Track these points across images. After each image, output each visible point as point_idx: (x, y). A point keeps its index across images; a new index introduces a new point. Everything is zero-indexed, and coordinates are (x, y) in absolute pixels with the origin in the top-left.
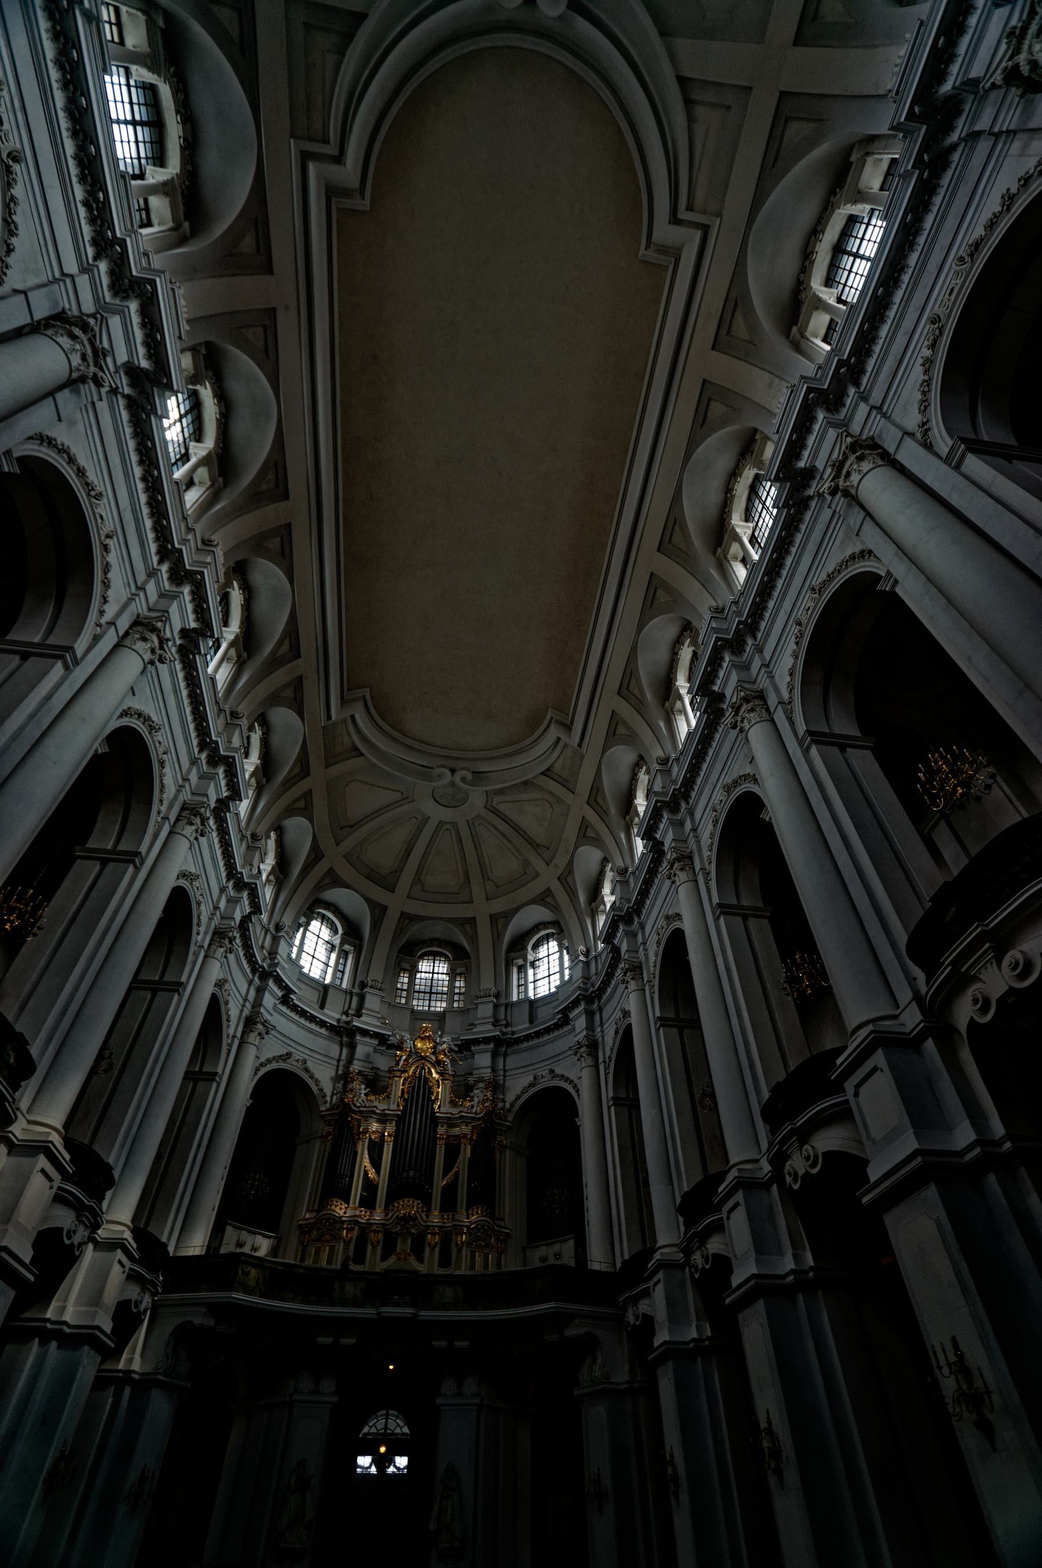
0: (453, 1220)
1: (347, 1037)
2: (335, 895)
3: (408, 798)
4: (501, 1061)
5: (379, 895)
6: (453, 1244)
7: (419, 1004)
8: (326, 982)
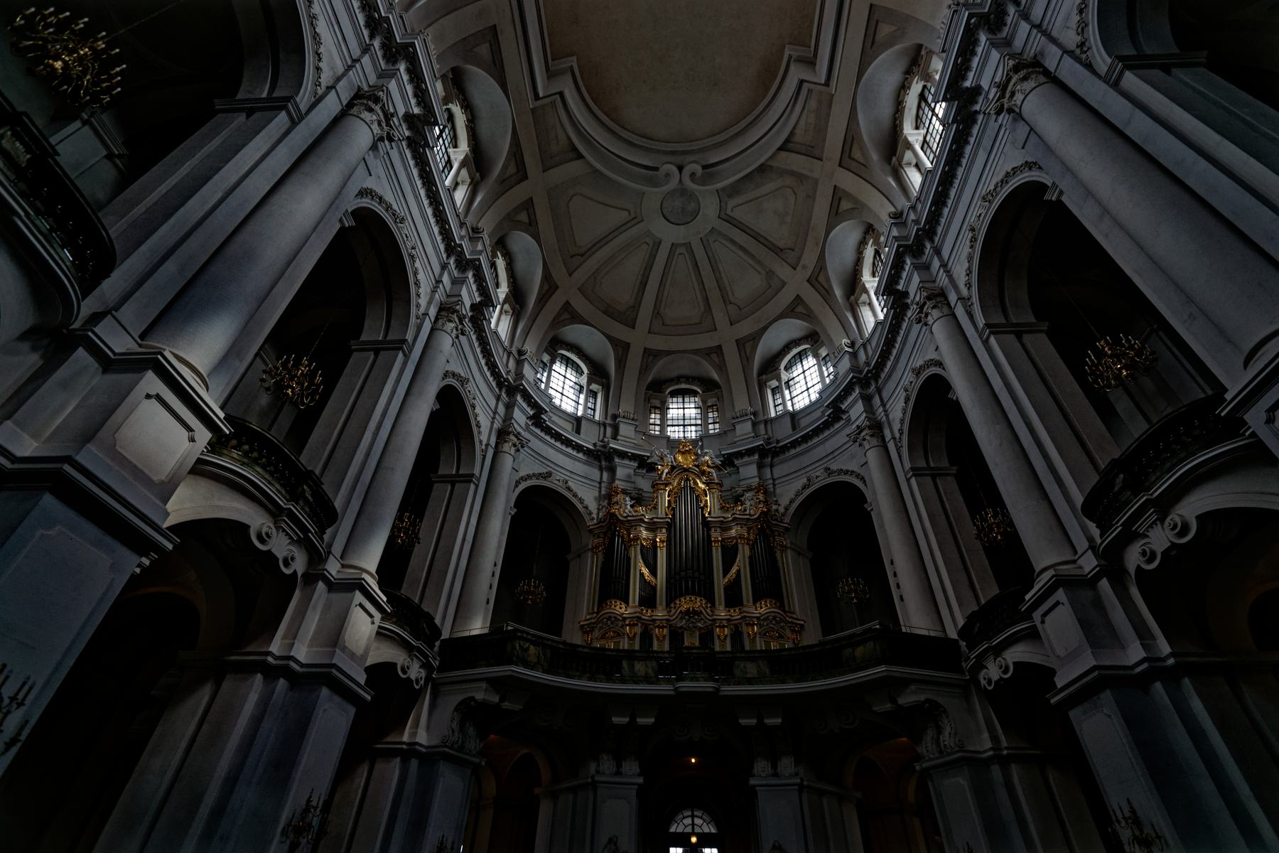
0: (740, 613)
2: (576, 333)
3: (636, 218)
4: (768, 471)
6: (745, 635)
7: (674, 433)
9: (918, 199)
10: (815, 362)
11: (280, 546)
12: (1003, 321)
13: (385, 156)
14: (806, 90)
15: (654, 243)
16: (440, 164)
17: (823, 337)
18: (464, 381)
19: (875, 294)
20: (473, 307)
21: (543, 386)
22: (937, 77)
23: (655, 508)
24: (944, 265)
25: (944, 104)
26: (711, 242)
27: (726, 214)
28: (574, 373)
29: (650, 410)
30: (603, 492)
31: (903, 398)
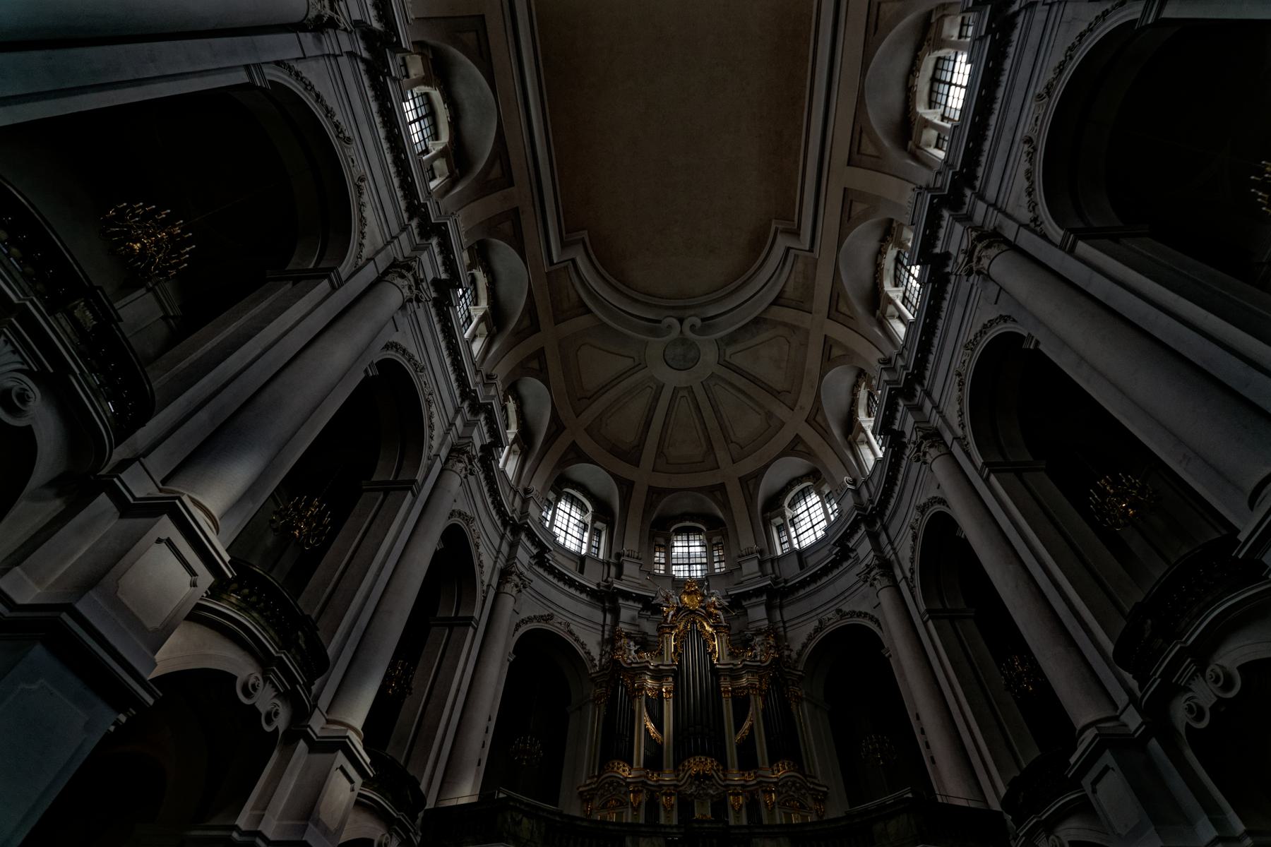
1: (609, 603)
2: (581, 471)
5: (626, 470)
6: (762, 805)
7: (680, 572)
8: (583, 553)
9: (904, 347)
10: (819, 499)
11: (265, 700)
12: (1001, 460)
13: (412, 314)
14: (793, 255)
15: (657, 387)
16: (461, 320)
17: (824, 475)
18: (469, 520)
19: (873, 433)
20: (483, 448)
21: (547, 524)
22: (910, 244)
23: (661, 654)
24: (936, 407)
25: (918, 267)
26: (711, 385)
27: (725, 360)
28: (579, 511)
29: (655, 548)
30: (606, 636)
31: (910, 535)
